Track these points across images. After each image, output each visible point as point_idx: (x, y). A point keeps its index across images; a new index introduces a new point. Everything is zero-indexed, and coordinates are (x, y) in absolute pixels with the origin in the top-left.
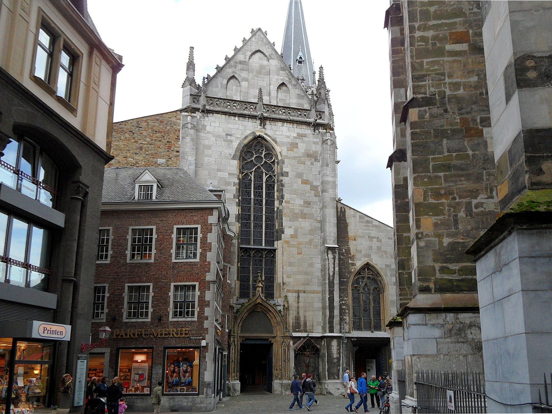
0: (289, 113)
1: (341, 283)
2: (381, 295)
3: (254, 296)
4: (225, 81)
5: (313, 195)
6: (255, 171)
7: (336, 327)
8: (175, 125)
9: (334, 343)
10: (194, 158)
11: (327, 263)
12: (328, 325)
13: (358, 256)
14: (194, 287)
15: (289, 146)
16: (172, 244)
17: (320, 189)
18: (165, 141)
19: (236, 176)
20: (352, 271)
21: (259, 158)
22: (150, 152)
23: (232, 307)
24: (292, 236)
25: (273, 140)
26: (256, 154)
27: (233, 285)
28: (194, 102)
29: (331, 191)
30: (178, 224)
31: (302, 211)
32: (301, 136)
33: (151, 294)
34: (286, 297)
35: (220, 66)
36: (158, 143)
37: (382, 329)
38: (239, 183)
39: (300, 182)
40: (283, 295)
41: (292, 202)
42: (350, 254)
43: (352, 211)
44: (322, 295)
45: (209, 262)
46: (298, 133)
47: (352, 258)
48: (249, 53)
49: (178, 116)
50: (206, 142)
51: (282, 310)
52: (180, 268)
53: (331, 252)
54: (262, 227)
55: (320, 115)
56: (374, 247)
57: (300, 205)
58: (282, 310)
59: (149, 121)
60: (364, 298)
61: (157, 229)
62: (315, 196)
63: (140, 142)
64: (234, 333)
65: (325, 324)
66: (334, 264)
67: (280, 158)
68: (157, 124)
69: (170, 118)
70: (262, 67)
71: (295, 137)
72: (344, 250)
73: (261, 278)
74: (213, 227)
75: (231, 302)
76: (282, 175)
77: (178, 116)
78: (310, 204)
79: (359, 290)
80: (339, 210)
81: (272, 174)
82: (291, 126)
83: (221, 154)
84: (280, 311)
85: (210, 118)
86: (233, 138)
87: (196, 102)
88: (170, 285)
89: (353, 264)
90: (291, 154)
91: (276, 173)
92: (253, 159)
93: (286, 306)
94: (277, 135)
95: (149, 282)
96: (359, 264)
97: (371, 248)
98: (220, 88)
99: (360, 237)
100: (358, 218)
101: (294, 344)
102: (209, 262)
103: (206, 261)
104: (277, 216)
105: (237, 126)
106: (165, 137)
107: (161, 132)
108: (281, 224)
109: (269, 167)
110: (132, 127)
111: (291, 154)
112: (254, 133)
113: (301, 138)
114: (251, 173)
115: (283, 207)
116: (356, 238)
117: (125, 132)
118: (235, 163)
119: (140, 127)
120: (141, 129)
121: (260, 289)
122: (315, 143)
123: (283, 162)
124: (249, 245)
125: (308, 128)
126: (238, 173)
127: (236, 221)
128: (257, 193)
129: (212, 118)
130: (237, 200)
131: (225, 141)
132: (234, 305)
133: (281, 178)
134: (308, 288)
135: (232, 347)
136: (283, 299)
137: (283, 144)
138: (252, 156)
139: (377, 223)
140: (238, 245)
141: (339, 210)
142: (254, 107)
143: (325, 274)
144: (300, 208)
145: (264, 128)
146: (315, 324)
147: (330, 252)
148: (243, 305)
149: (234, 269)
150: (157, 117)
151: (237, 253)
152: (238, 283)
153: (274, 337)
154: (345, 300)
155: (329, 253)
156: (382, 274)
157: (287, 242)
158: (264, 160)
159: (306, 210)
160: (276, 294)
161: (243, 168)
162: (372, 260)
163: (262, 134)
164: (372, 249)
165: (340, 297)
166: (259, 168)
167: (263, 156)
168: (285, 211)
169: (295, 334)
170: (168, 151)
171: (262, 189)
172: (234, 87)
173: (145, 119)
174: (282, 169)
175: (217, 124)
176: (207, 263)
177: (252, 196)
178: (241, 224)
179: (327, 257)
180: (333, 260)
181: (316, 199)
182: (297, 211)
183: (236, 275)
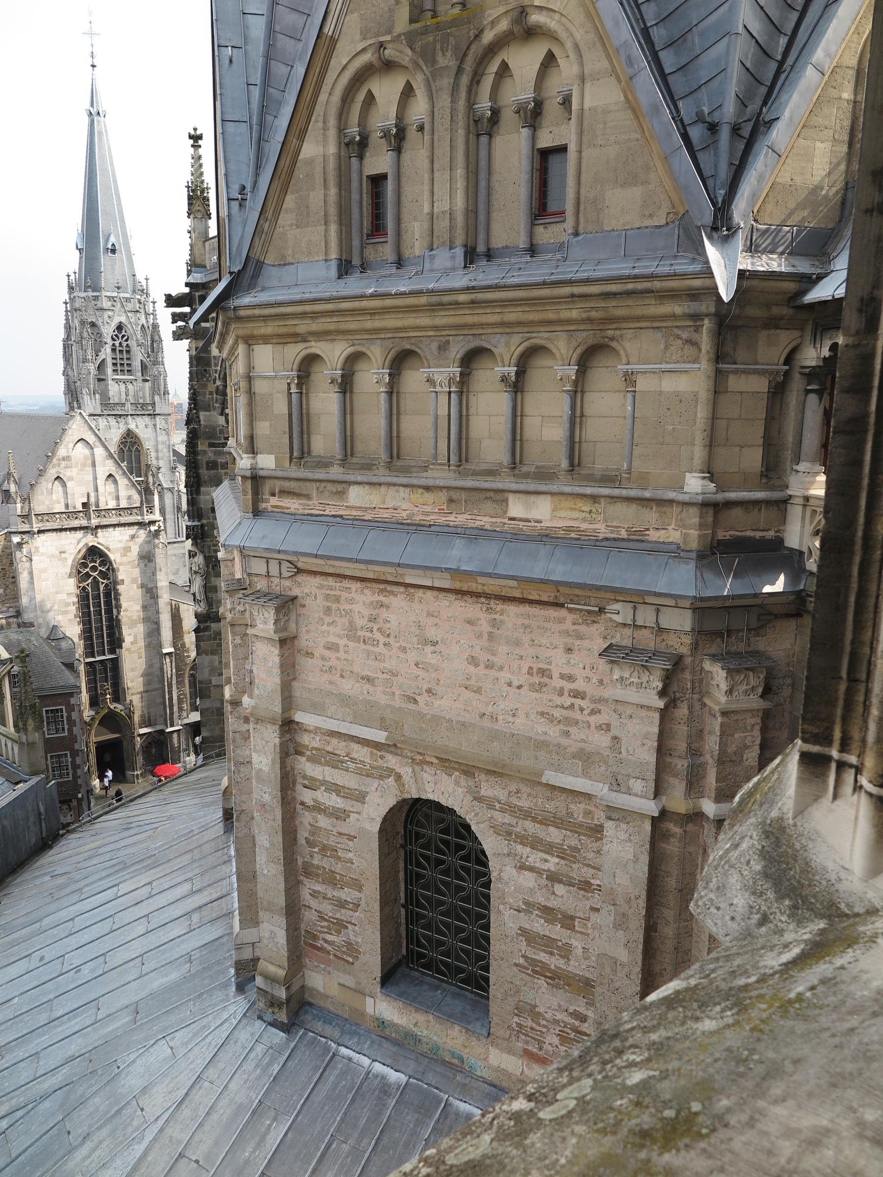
24: (132, 643)
25: (107, 548)
32: (133, 537)
41: (129, 609)
67: (115, 566)
71: (127, 541)
90: (125, 559)
105: (69, 541)
108: (121, 633)
111: (125, 559)
112: (87, 544)
129: (43, 537)
131: (59, 559)
157: (128, 650)
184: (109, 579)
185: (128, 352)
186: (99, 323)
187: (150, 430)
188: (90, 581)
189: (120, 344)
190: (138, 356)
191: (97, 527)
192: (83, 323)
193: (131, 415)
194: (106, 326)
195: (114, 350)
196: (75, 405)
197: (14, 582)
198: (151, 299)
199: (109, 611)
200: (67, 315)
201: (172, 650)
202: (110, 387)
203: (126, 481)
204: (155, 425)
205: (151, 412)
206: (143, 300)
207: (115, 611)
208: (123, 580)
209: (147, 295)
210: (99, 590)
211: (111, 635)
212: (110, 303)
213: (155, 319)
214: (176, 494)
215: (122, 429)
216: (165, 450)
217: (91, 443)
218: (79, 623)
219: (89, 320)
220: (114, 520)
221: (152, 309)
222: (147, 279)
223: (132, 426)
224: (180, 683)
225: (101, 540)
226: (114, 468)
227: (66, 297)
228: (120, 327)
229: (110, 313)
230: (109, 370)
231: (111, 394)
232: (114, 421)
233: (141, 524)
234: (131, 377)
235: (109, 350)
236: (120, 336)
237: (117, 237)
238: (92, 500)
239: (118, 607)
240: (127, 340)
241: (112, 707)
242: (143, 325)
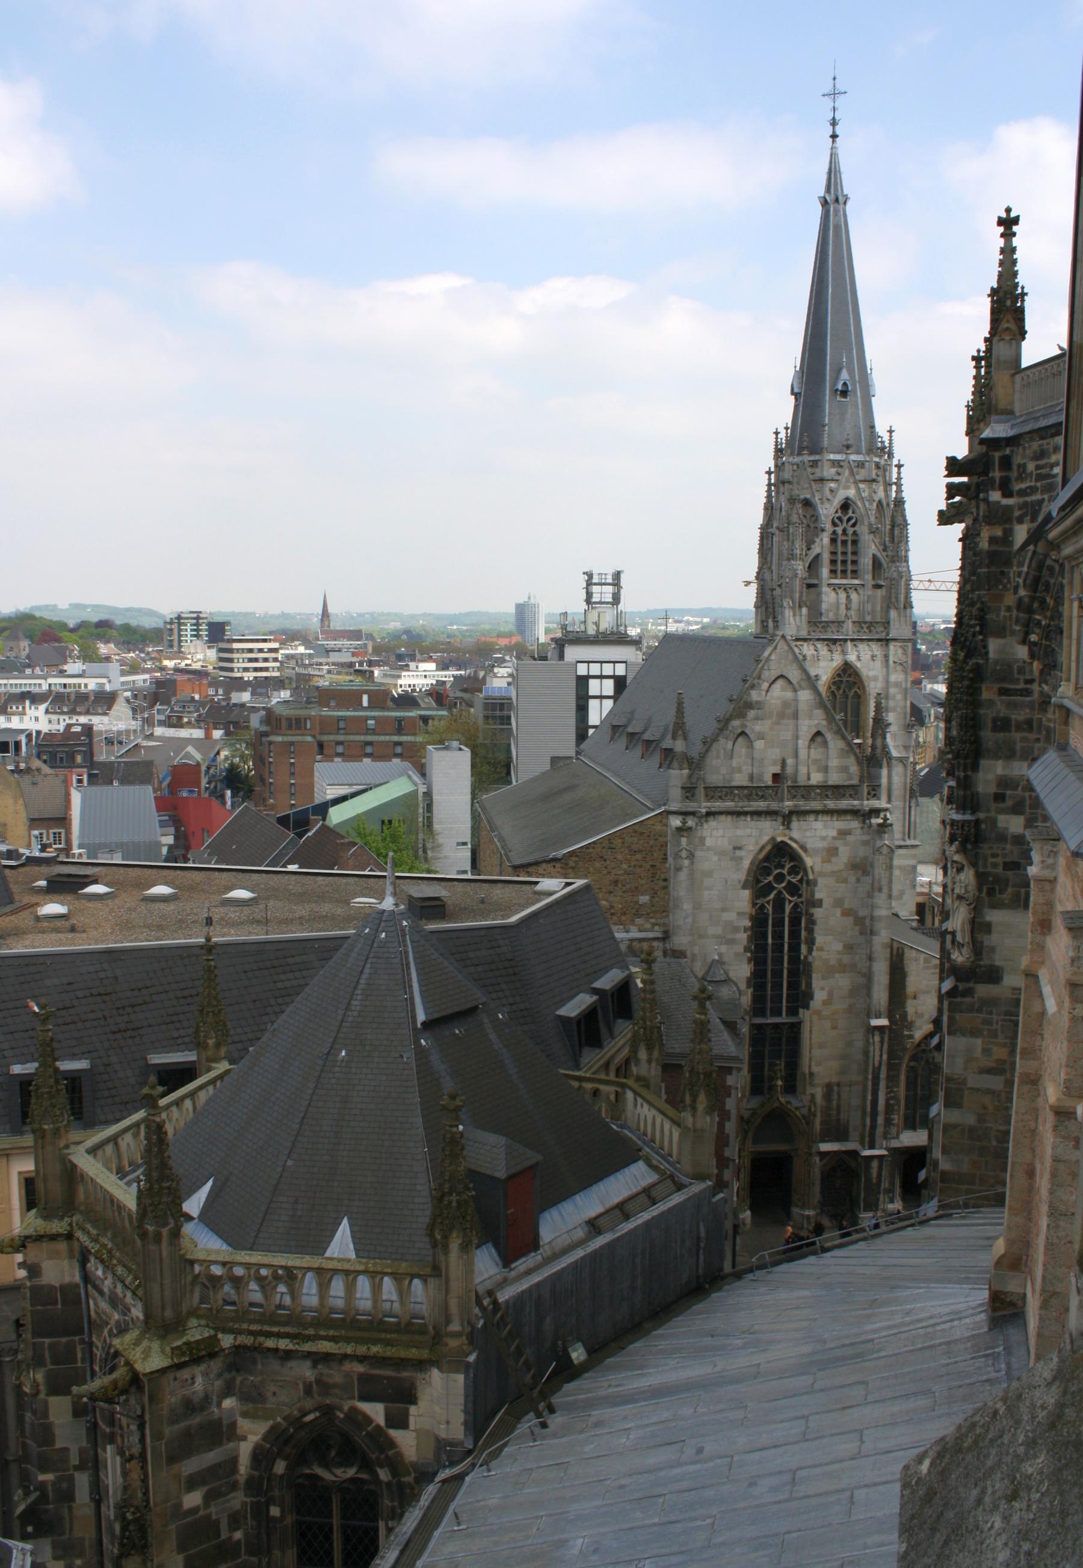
13: (918, 1022)
24: (825, 1003)
28: (687, 797)
32: (843, 833)
38: (752, 928)
42: (906, 1020)
47: (910, 1026)
50: (706, 866)
57: (839, 953)
67: (811, 877)
71: (834, 838)
80: (895, 952)
83: (726, 882)
86: (743, 853)
89: (911, 1037)
90: (828, 867)
100: (922, 961)
105: (749, 831)
108: (809, 985)
109: (793, 889)
112: (773, 839)
118: (746, 894)
129: (712, 823)
131: (733, 859)
141: (895, 952)
157: (818, 1012)
168: (817, 964)
174: (813, 894)
182: (832, 962)
184: (800, 896)
185: (855, 542)
186: (816, 500)
187: (878, 664)
188: (772, 896)
189: (844, 531)
190: (870, 548)
191: (791, 813)
192: (792, 501)
193: (852, 640)
194: (827, 505)
195: (833, 541)
196: (771, 624)
197: (665, 888)
198: (895, 462)
199: (795, 948)
200: (769, 491)
201: (884, 1022)
202: (824, 598)
203: (841, 744)
204: (886, 656)
205: (883, 636)
206: (882, 462)
207: (804, 949)
208: (821, 901)
209: (891, 455)
210: (784, 912)
211: (793, 985)
212: (833, 470)
213: (899, 491)
214: (910, 768)
215: (837, 660)
216: (899, 697)
217: (794, 681)
218: (749, 961)
219: (802, 497)
220: (816, 805)
221: (895, 475)
222: (891, 432)
223: (852, 657)
224: (892, 1079)
225: (795, 834)
226: (824, 723)
227: (771, 464)
228: (846, 506)
229: (833, 485)
230: (825, 572)
231: (824, 606)
232: (825, 648)
233: (854, 813)
234: (856, 582)
235: (826, 540)
236: (845, 519)
237: (851, 372)
238: (789, 770)
239: (811, 942)
240: (854, 525)
241: (783, 1100)
242: (880, 502)
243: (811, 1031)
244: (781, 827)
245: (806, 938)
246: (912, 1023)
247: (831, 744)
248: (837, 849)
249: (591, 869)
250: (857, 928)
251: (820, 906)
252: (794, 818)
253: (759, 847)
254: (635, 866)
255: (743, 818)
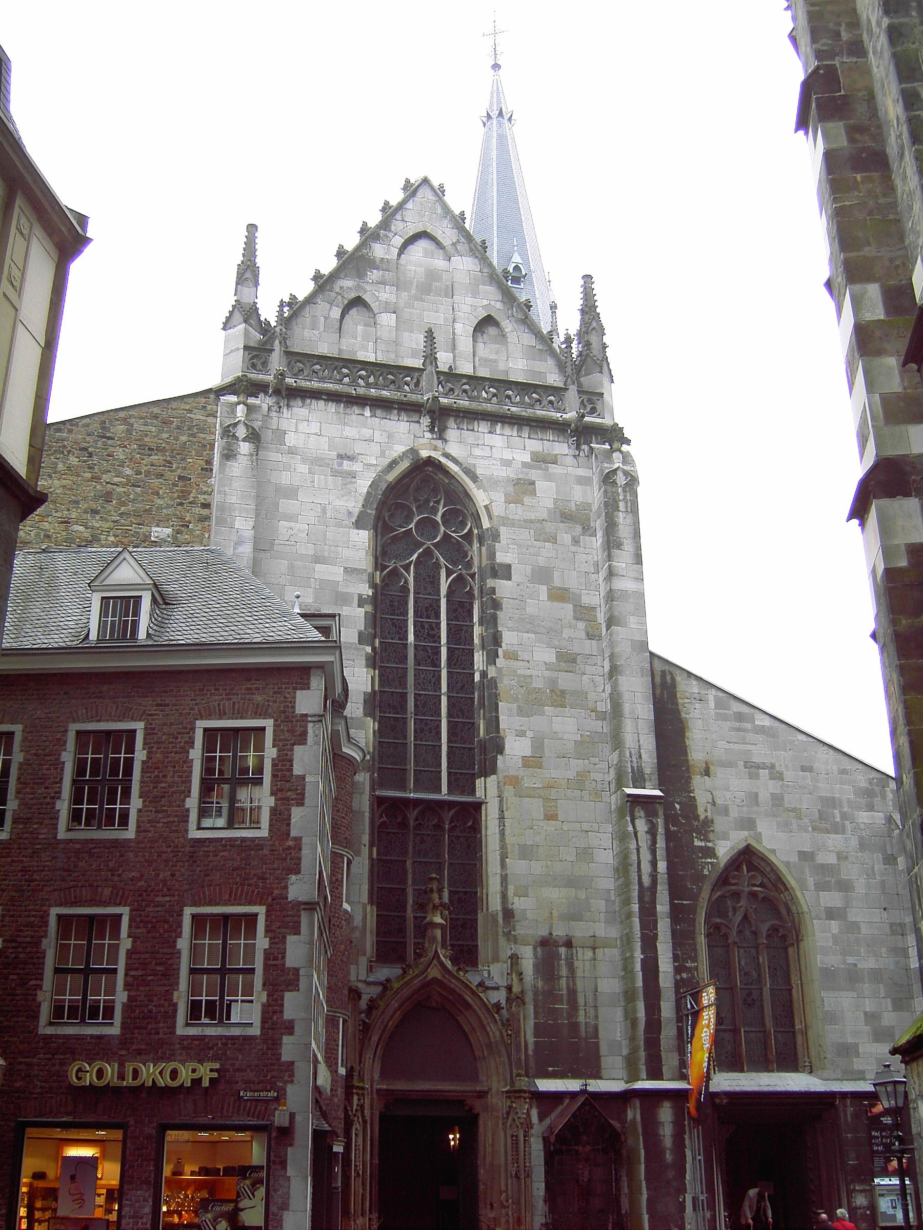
0: (509, 397)
1: (676, 913)
2: (790, 950)
3: (418, 956)
4: (336, 313)
5: (583, 635)
6: (418, 562)
7: (670, 1060)
8: (202, 430)
9: (666, 1113)
10: (252, 523)
11: (633, 846)
12: (642, 1054)
13: (720, 824)
14: (252, 919)
15: (511, 489)
16: (188, 781)
17: (601, 618)
18: (173, 477)
19: (365, 577)
20: (706, 872)
21: (428, 525)
22: (130, 507)
23: (355, 994)
26: (420, 513)
27: (357, 921)
29: (632, 621)
30: (209, 717)
31: (553, 682)
32: (541, 460)
33: (126, 943)
34: (515, 959)
35: (322, 272)
36: (155, 482)
37: (801, 1064)
38: (375, 600)
39: (544, 595)
40: (506, 951)
42: (697, 817)
43: (694, 683)
44: (623, 953)
45: (298, 840)
46: (532, 453)
48: (398, 241)
49: (209, 407)
50: (285, 479)
51: (503, 1002)
52: (211, 858)
53: (642, 814)
54: (439, 733)
55: (590, 401)
56: (764, 796)
57: (548, 666)
58: (503, 1002)
59: (132, 421)
60: (743, 963)
61: (148, 733)
62: (590, 637)
63: (105, 477)
64: (361, 1079)
65: (634, 1050)
66: (653, 851)
67: (486, 524)
68: (154, 429)
69: (190, 411)
70: (432, 275)
71: (525, 465)
72: (678, 806)
73: (441, 898)
74: (310, 725)
75: (353, 977)
76: (495, 574)
77: (209, 407)
78: (574, 661)
79: (726, 936)
81: (464, 572)
82: (515, 434)
83: (324, 511)
84: (498, 1006)
85: (296, 410)
86: (357, 467)
87: (259, 366)
88: (180, 914)
89: (710, 852)
90: (517, 512)
91: (475, 569)
92: (412, 526)
93: (516, 989)
94: (476, 457)
95: (119, 905)
96: (724, 850)
97: (754, 798)
98: (322, 328)
99: (722, 764)
100: (712, 704)
101: (541, 1118)
102: (298, 840)
103: (288, 834)
104: (481, 698)
105: (367, 432)
106: (174, 466)
107: (160, 450)
108: (494, 723)
110: (88, 439)
111: (517, 512)
112: (413, 451)
113: (543, 466)
114: (407, 568)
115: (499, 670)
116: (712, 768)
117: (69, 452)
118: (363, 537)
119: (109, 438)
120: (110, 442)
121: (438, 933)
122: (584, 481)
123: (496, 536)
124: (403, 787)
125: (561, 439)
126: (370, 570)
127: (366, 715)
128: (423, 627)
130: (369, 649)
131: (335, 473)
132: (360, 985)
133: (490, 583)
134: (580, 931)
135: (357, 1126)
136: (506, 966)
137: (494, 483)
138: (409, 519)
139: (767, 722)
140: (373, 789)
141: (658, 679)
142: (415, 381)
143: (627, 884)
144: (547, 674)
145: (441, 437)
146: (603, 1049)
147: (640, 813)
148: (385, 985)
149: (361, 866)
150: (156, 410)
151: (367, 815)
152: (371, 913)
153: (482, 1095)
154: (688, 970)
155: (637, 814)
156: (792, 882)
157: (515, 781)
158: (442, 529)
159: (565, 681)
160: (484, 949)
161: (384, 553)
162: (758, 838)
163: (437, 455)
164: (757, 804)
165: (675, 958)
166: (428, 553)
167: (438, 518)
168: (505, 685)
169: (546, 1085)
170: (181, 504)
171: (438, 616)
172: (360, 328)
173: (122, 415)
174: (492, 555)
175: (314, 428)
176: (290, 843)
177: (411, 638)
178: (380, 723)
179: (630, 828)
180: (649, 837)
181: (590, 647)
182: (538, 684)
183: (365, 887)
184: (469, 565)
208: (509, 566)
225: (454, 449)
243: (502, 818)
244: (428, 435)
245: (482, 638)
246: (708, 822)
247: (512, 337)
248: (533, 483)
249: (60, 466)
250: (581, 625)
251: (509, 578)
252: (451, 423)
253: (387, 461)
254: (148, 473)
255: (357, 410)
